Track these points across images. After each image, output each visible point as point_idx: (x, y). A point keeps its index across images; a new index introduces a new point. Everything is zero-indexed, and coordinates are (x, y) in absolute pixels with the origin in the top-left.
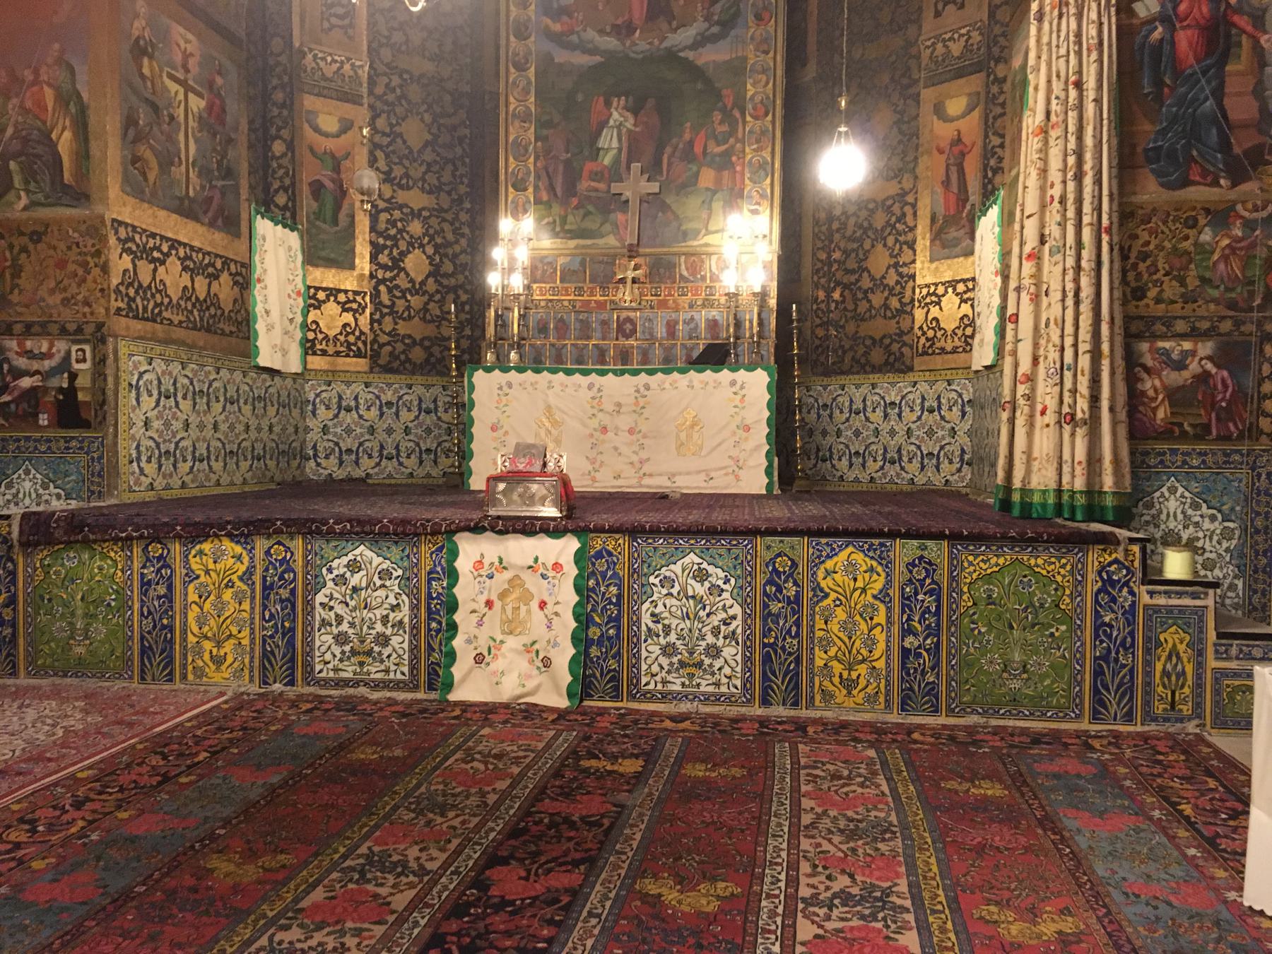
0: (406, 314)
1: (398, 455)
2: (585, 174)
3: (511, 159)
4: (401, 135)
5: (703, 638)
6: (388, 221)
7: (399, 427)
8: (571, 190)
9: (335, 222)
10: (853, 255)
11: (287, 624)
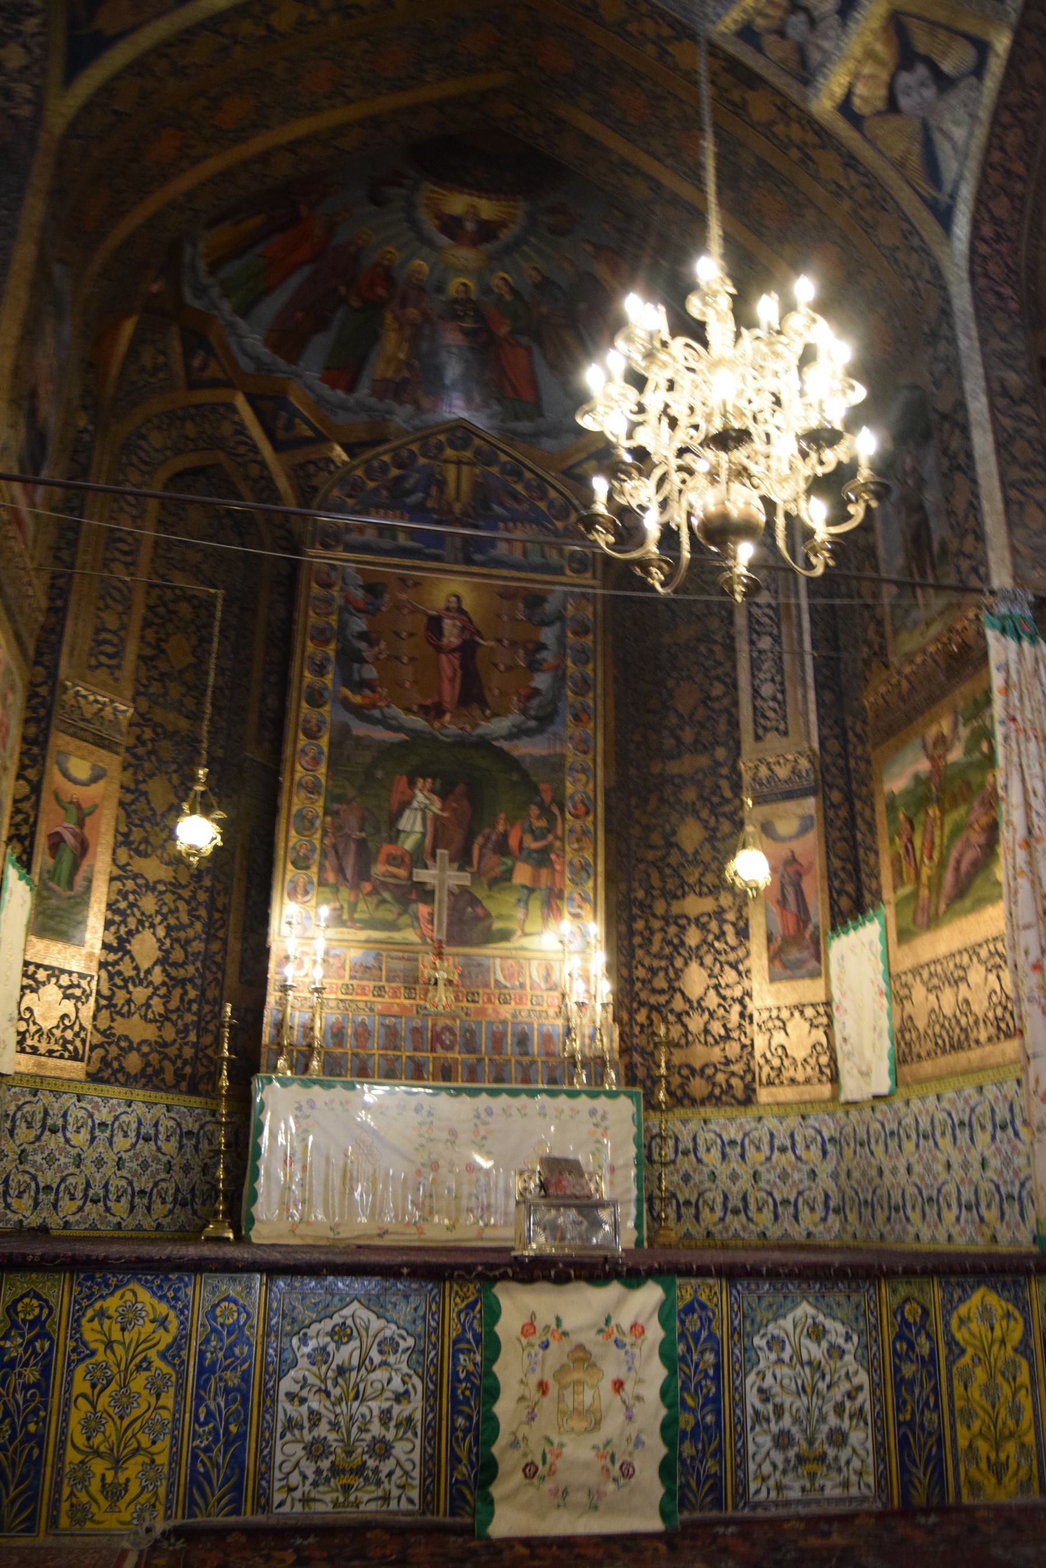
0: (125, 1009)
1: (106, 1197)
2: (382, 857)
3: (293, 833)
4: (145, 794)
5: (823, 1418)
6: (119, 892)
7: (110, 1157)
8: (363, 873)
9: (70, 884)
10: (662, 974)
11: (233, 1429)
